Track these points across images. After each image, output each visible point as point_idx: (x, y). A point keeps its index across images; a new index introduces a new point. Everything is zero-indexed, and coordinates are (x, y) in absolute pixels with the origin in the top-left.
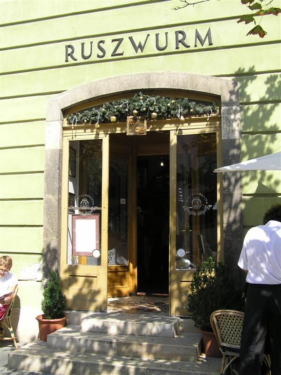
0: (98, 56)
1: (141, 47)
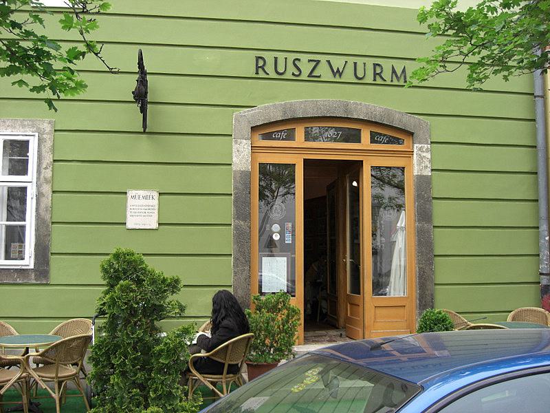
0: (293, 74)
1: (339, 73)
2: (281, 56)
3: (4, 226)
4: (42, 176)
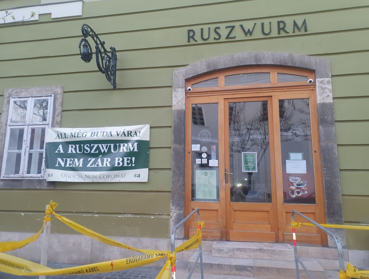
0: (215, 39)
1: (250, 33)
2: (205, 28)
3: (38, 153)
4: (55, 121)
